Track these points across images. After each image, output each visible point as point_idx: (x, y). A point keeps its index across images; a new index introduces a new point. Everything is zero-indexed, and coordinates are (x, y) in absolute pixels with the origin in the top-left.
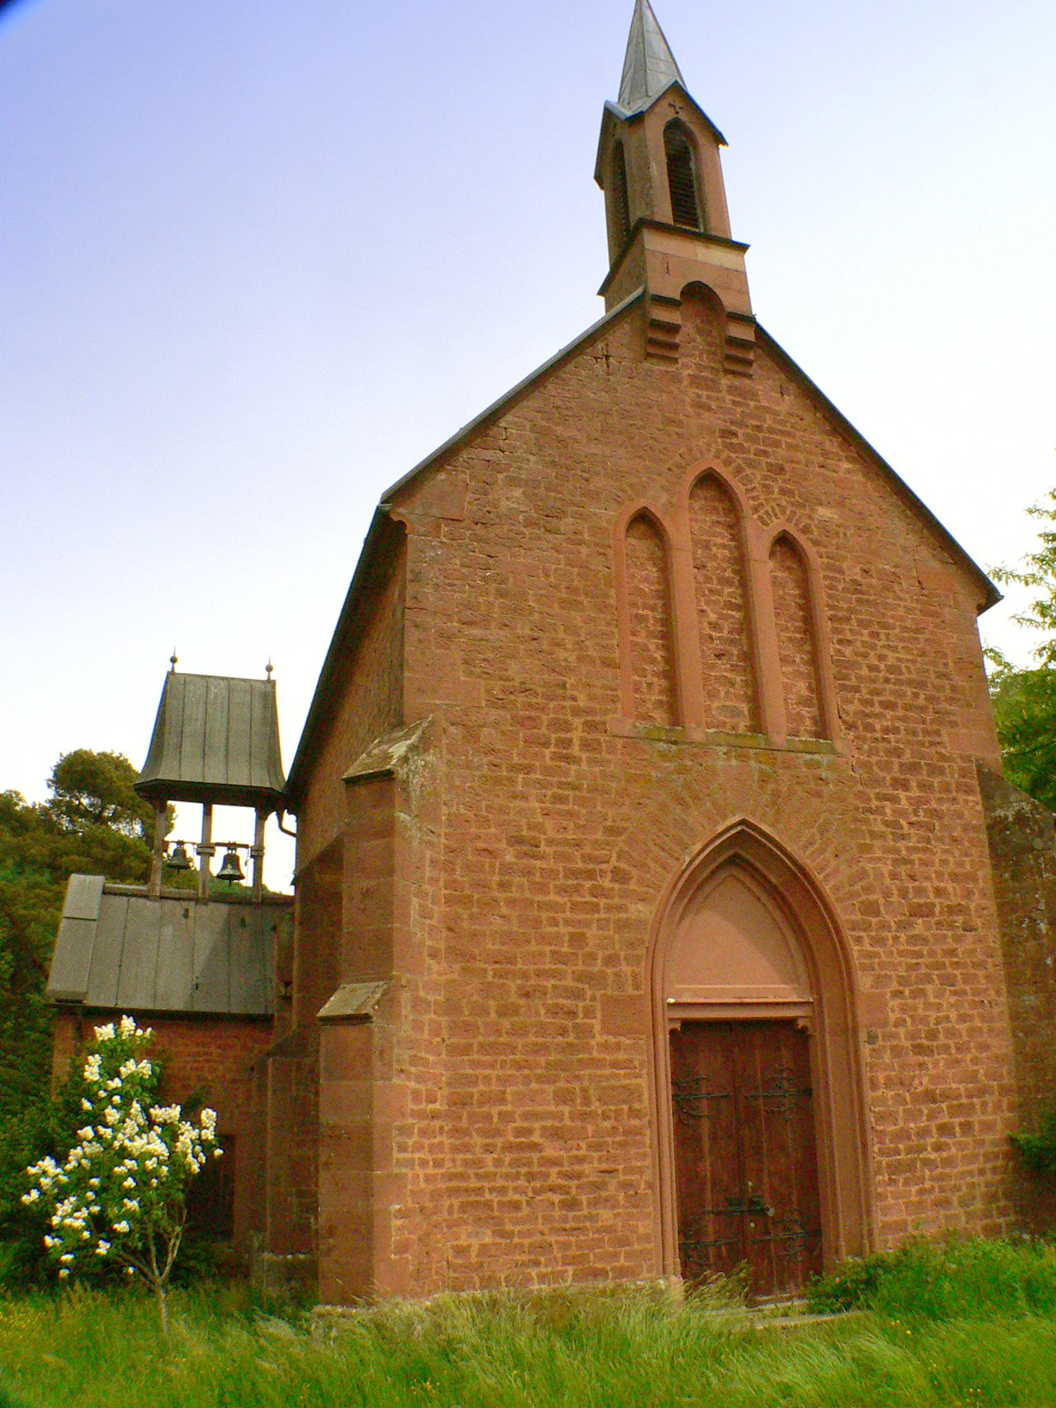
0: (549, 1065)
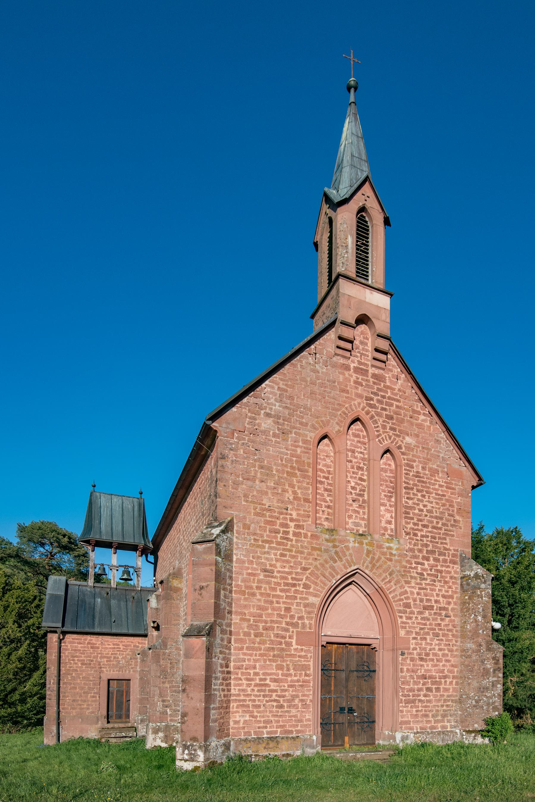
0: (274, 656)
